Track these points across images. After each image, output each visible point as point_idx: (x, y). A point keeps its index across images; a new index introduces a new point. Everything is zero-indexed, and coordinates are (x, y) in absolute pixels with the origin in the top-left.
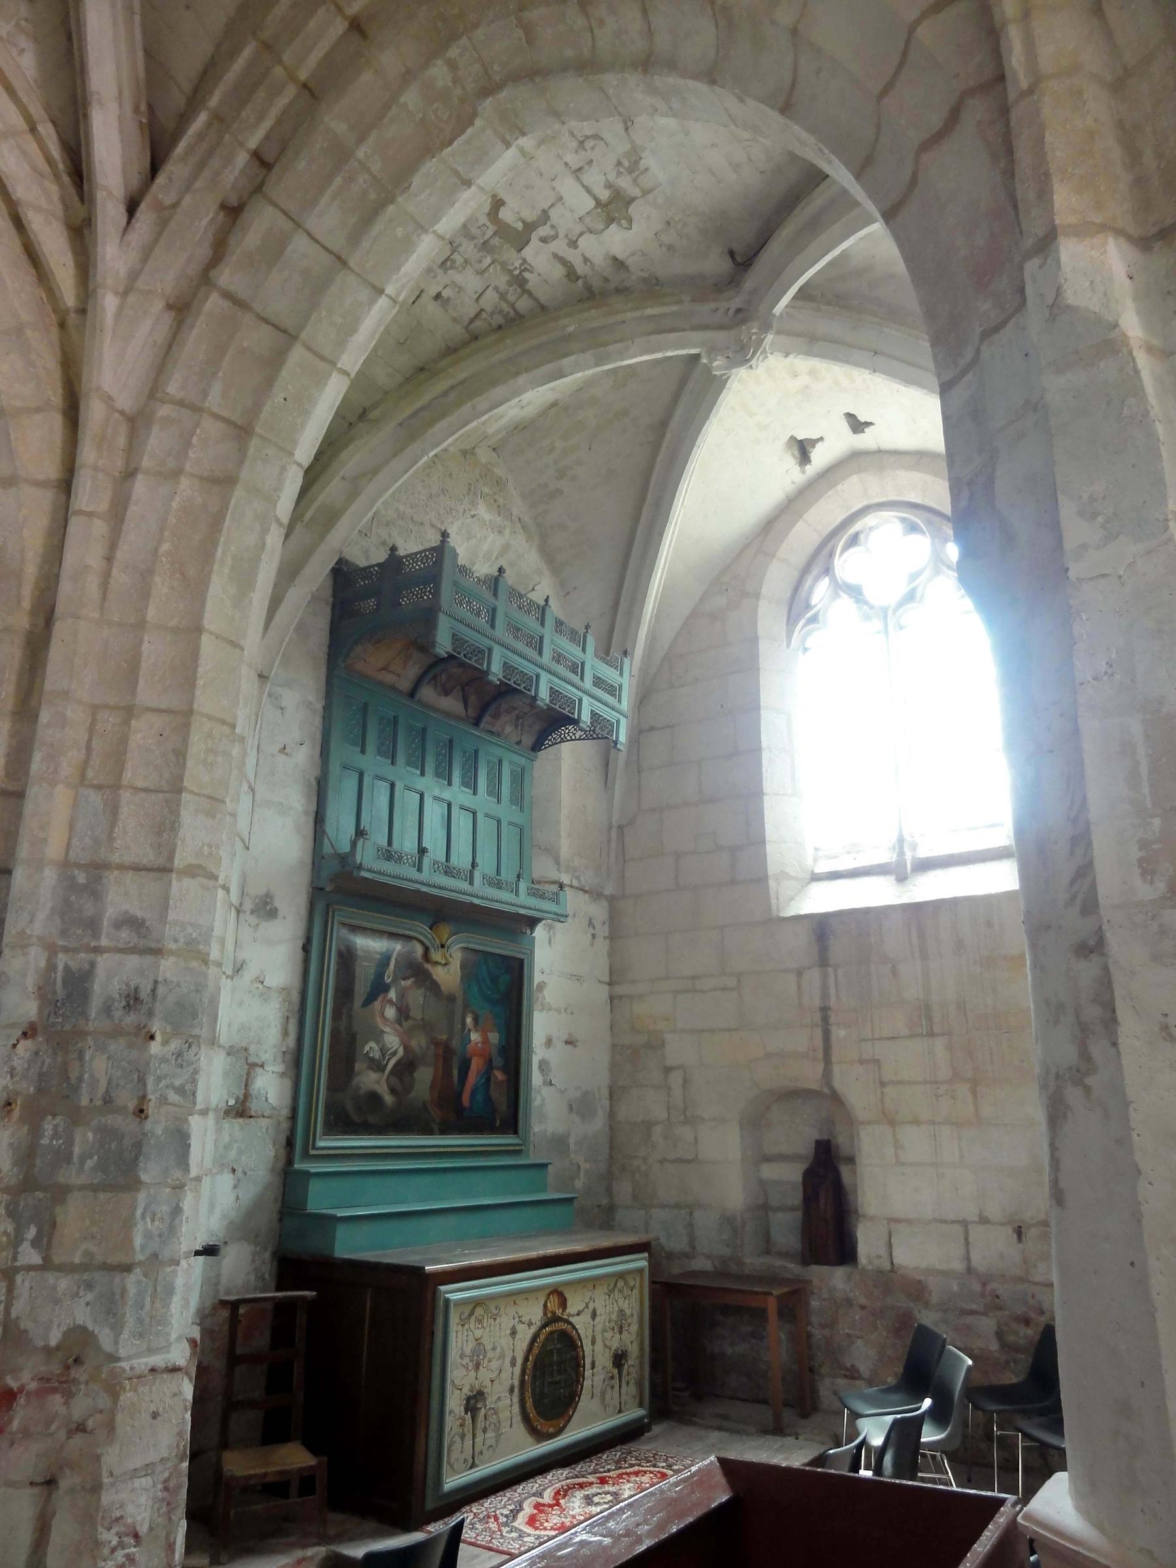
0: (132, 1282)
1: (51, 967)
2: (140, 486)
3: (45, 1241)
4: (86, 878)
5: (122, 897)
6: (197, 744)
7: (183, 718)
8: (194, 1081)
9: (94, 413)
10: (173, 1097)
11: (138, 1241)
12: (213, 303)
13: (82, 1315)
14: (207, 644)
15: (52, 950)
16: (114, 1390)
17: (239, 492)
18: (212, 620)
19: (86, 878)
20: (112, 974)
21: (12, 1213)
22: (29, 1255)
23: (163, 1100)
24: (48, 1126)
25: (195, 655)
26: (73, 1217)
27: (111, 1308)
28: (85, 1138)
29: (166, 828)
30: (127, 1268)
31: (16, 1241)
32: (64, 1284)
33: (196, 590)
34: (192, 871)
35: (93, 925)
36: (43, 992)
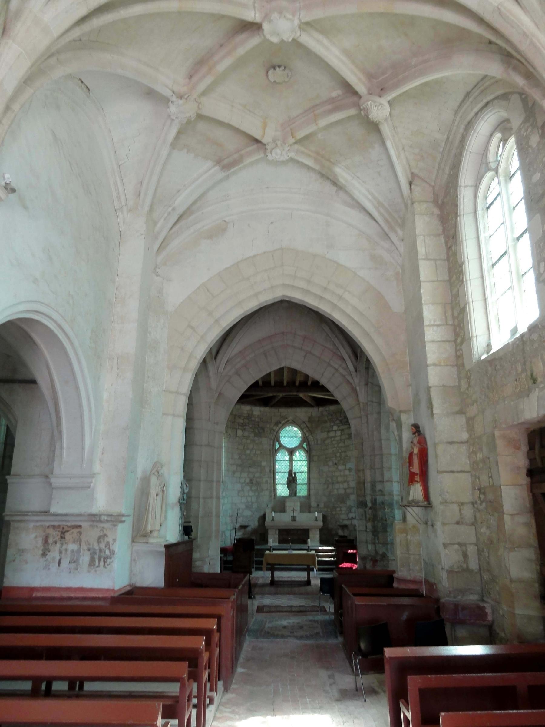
0: (389, 546)
1: (372, 498)
2: (369, 417)
3: (378, 539)
4: (373, 485)
5: (379, 487)
6: (385, 460)
7: (382, 455)
8: (394, 515)
9: (361, 405)
10: (391, 518)
11: (389, 540)
12: (370, 385)
13: (384, 550)
14: (383, 441)
15: (372, 496)
16: (388, 561)
17: (382, 414)
18: (383, 437)
19: (373, 485)
20: (379, 499)
21: (373, 535)
22: (377, 541)
23: (389, 519)
24: (376, 522)
25: (381, 444)
26: (380, 535)
27: (387, 549)
28: (380, 524)
29: (382, 475)
30: (388, 544)
31: (375, 539)
32: (381, 545)
33: (380, 433)
34: (388, 481)
35: (375, 491)
36: (372, 502)
